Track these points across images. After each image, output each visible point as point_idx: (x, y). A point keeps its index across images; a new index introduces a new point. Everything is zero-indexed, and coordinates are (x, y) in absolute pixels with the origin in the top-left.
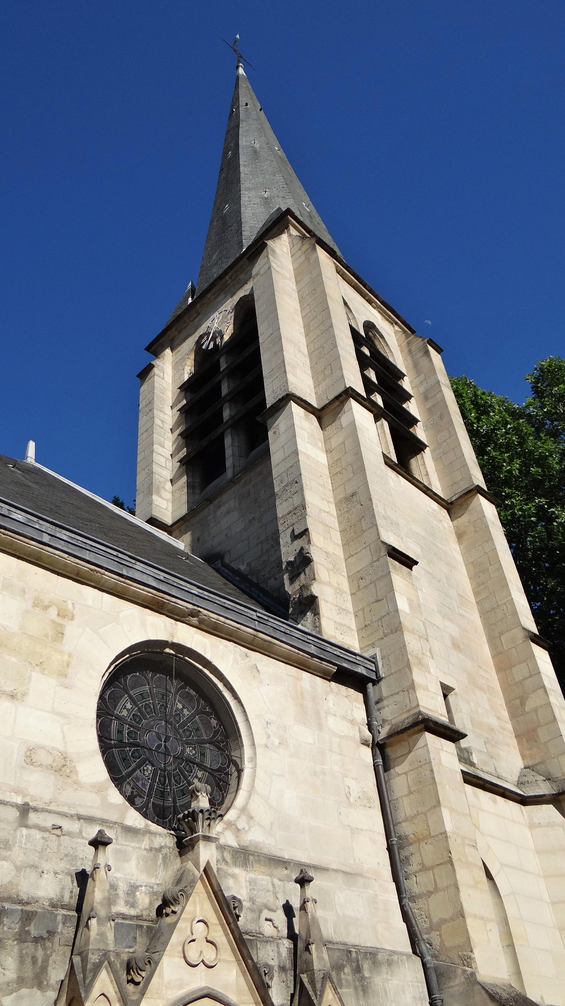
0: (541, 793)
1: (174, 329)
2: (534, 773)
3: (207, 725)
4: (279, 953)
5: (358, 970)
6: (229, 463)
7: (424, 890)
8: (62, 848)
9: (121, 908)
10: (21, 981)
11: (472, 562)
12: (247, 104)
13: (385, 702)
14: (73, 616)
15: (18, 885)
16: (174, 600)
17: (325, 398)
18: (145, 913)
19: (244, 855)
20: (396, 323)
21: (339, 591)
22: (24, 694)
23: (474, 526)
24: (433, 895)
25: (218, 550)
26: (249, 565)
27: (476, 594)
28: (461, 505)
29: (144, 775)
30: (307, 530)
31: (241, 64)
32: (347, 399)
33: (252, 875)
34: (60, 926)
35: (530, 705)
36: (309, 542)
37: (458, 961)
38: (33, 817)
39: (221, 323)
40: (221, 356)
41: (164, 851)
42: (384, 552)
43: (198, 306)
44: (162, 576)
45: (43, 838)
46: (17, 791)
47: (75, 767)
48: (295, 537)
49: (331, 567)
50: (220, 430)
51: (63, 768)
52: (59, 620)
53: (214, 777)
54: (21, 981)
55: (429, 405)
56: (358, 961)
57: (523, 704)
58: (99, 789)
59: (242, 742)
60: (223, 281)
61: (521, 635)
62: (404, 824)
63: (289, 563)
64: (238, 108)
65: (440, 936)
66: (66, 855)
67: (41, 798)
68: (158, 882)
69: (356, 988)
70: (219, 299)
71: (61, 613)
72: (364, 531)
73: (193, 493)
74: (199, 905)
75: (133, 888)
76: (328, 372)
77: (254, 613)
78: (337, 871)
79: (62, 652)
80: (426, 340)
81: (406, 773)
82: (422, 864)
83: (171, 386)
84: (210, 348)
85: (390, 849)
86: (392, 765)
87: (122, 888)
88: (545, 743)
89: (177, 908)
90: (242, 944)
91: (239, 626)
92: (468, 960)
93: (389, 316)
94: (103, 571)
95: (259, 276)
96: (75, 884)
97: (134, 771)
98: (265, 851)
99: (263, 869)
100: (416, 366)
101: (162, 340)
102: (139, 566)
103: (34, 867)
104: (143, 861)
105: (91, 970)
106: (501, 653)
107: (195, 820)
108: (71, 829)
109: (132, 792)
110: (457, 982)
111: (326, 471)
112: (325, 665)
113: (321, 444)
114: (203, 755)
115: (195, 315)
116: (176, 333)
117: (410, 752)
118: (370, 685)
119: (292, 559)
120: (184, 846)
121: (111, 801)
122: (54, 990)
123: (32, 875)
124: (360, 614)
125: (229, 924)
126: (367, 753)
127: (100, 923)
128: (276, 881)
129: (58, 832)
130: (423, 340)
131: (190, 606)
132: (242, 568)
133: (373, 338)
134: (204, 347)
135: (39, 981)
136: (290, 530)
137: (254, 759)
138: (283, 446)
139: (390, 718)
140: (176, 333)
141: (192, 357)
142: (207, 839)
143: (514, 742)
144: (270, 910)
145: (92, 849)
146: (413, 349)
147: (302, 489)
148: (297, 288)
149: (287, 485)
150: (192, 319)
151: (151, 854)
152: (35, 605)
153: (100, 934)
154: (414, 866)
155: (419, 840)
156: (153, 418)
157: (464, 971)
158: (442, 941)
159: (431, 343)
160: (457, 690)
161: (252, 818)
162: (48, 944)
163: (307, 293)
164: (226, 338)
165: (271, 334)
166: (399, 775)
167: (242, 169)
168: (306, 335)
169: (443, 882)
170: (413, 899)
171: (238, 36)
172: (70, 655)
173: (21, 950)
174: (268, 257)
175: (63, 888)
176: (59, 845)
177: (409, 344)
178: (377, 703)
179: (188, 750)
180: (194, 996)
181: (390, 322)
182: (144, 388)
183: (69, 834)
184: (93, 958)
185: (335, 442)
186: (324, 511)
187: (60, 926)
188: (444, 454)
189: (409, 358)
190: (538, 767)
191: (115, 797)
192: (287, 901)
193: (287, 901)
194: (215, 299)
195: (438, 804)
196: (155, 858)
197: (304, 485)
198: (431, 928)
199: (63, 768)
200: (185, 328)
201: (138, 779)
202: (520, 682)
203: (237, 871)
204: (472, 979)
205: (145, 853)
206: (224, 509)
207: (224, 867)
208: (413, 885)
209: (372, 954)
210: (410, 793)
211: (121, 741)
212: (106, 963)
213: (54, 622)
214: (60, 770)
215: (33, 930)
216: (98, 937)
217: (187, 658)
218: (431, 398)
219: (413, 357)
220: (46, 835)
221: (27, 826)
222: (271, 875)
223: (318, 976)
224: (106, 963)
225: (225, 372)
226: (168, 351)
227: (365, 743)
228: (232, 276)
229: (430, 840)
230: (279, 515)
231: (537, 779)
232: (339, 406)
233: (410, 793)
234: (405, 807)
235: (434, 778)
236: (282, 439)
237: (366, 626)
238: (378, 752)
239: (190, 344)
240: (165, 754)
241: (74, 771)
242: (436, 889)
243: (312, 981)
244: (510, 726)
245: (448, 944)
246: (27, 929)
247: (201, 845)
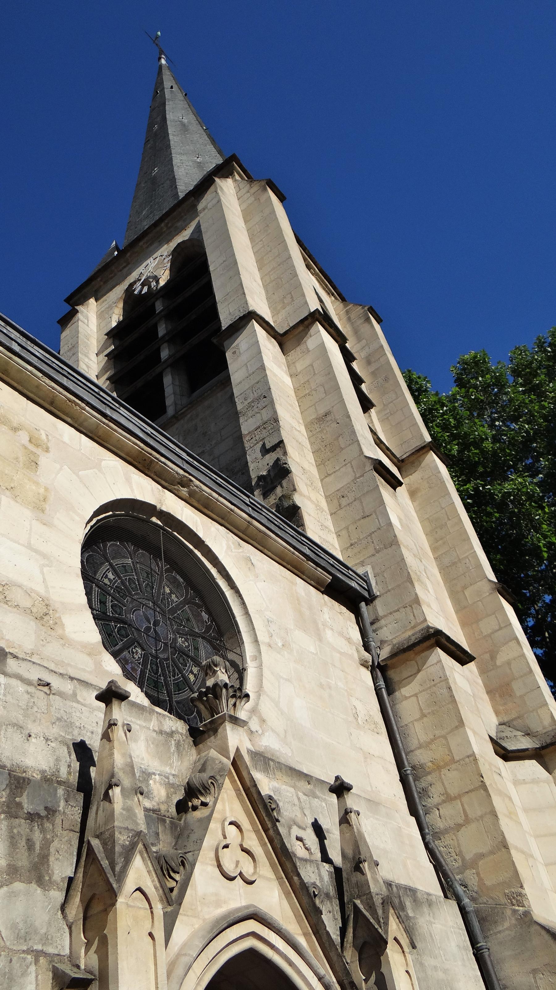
0: (524, 747)
1: (99, 279)
2: (510, 729)
3: (198, 617)
6: (169, 401)
7: (451, 823)
8: (53, 709)
12: (172, 87)
13: (383, 622)
16: (163, 459)
17: (286, 325)
18: (163, 808)
20: (333, 294)
21: (318, 507)
23: (428, 482)
24: (463, 829)
27: (434, 549)
28: (413, 463)
29: (133, 657)
30: (282, 442)
31: (163, 56)
32: (313, 323)
34: (62, 803)
35: (501, 659)
36: (285, 453)
37: (504, 900)
39: (157, 267)
40: (157, 299)
41: (177, 737)
42: (369, 466)
43: (129, 254)
44: (149, 430)
45: (28, 693)
47: (60, 618)
48: (265, 451)
49: (309, 483)
52: (31, 447)
54: (13, 872)
56: (400, 897)
57: (493, 657)
59: (242, 639)
60: (158, 229)
62: (418, 752)
63: (260, 478)
64: (163, 90)
65: (478, 874)
66: (59, 719)
67: (20, 646)
68: (173, 772)
70: (152, 248)
71: (33, 441)
72: (342, 449)
74: (228, 804)
76: (288, 300)
77: (247, 499)
79: (37, 483)
80: (366, 308)
81: (416, 695)
82: (446, 793)
83: (96, 334)
84: (143, 292)
85: (404, 780)
86: (396, 688)
88: (521, 696)
89: (208, 799)
90: (284, 858)
91: (233, 507)
92: (518, 898)
93: (326, 286)
94: (83, 405)
95: (206, 211)
96: (74, 756)
98: (282, 760)
99: (285, 778)
100: (356, 332)
101: (85, 290)
103: (19, 727)
104: (153, 743)
105: (121, 854)
106: (465, 607)
107: (217, 697)
108: (62, 689)
110: (507, 924)
111: (292, 393)
113: (285, 368)
114: (197, 649)
115: (125, 264)
116: (102, 283)
117: (419, 671)
118: (363, 604)
119: (265, 473)
120: (197, 736)
121: (106, 668)
122: (59, 889)
124: (344, 533)
125: (266, 831)
126: (366, 675)
128: (300, 794)
129: (46, 689)
130: (363, 308)
131: (181, 472)
134: (136, 292)
135: (38, 873)
137: (258, 657)
138: (246, 364)
139: (390, 638)
140: (102, 283)
141: (121, 305)
142: (235, 720)
143: (486, 697)
144: (300, 827)
145: (103, 705)
146: (353, 316)
147: (272, 403)
148: (246, 227)
149: (253, 402)
150: (121, 267)
151: (161, 738)
153: (125, 811)
155: (439, 768)
156: (78, 361)
157: (515, 911)
158: (481, 880)
159: (371, 310)
161: (264, 721)
162: (48, 825)
163: (259, 230)
164: (162, 283)
165: (224, 261)
166: (406, 698)
167: (171, 137)
168: (260, 269)
169: (475, 811)
170: (437, 835)
171: (159, 33)
172: (46, 489)
173: (11, 828)
174: (216, 192)
175: (58, 760)
176: (49, 705)
177: (347, 312)
178: (372, 623)
179: (180, 640)
180: (240, 914)
181: (326, 291)
182: (66, 334)
183: (61, 694)
184: (122, 839)
185: (300, 366)
186: (296, 429)
187: (62, 803)
188: (391, 414)
190: (515, 723)
192: (316, 819)
193: (316, 819)
194: (147, 247)
196: (166, 744)
197: (274, 399)
198: (461, 871)
200: (111, 278)
202: (489, 636)
204: (526, 919)
205: (154, 734)
208: (434, 820)
210: (423, 716)
211: (105, 613)
212: (140, 846)
214: (42, 618)
215: (27, 803)
216: (124, 812)
217: (175, 533)
218: (375, 362)
220: (31, 689)
222: (294, 787)
223: (378, 901)
224: (140, 846)
225: (163, 313)
226: (92, 301)
227: (364, 664)
229: (454, 766)
230: (244, 431)
231: (515, 734)
232: (303, 330)
233: (423, 716)
234: (417, 732)
235: (452, 696)
236: (244, 358)
237: (352, 545)
238: (379, 674)
239: (119, 291)
240: (155, 638)
242: (467, 821)
243: (371, 907)
244: (480, 682)
245: (488, 883)
246: (17, 799)
247: (228, 726)
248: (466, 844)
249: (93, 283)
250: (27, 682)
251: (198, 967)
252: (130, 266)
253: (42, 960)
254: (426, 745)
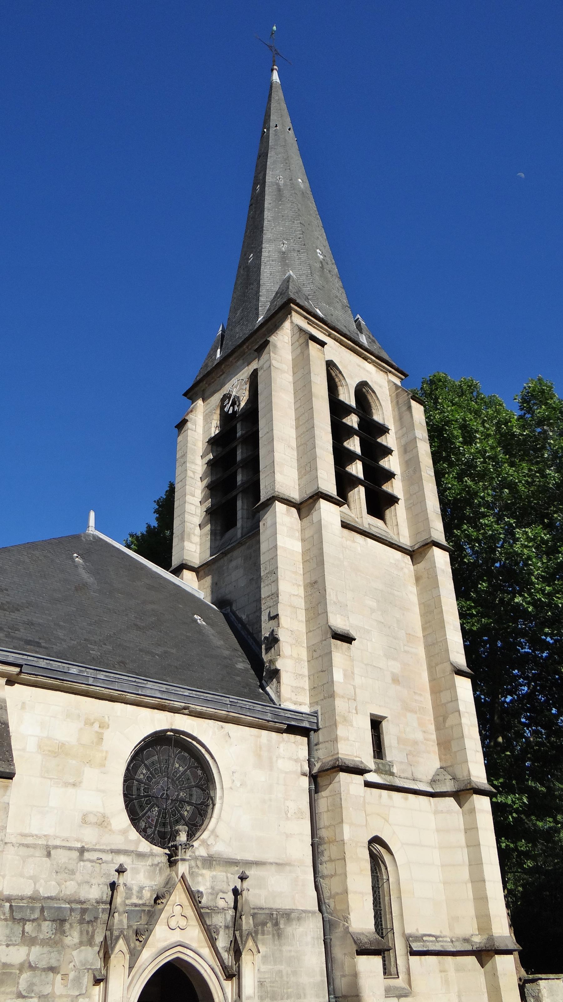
0: (445, 790)
1: (205, 382)
2: (445, 773)
3: (195, 775)
4: (225, 918)
5: (276, 924)
6: (239, 524)
8: (102, 870)
9: (135, 900)
10: (81, 943)
11: (423, 603)
12: (276, 126)
13: (320, 746)
14: (108, 726)
15: (79, 893)
16: (172, 702)
17: (305, 492)
18: (147, 902)
19: (210, 861)
20: (390, 372)
21: (298, 660)
22: (80, 782)
23: (428, 573)
24: (333, 877)
25: (228, 597)
26: (248, 616)
27: (424, 629)
28: (421, 553)
30: (278, 615)
31: (275, 67)
32: (317, 499)
33: (214, 873)
34: (101, 914)
35: (449, 723)
36: (278, 626)
37: (342, 918)
38: (87, 855)
40: (238, 422)
41: (160, 865)
42: (329, 635)
43: (223, 366)
44: (164, 688)
45: (92, 866)
46: (78, 840)
49: (294, 642)
50: (234, 493)
51: (103, 823)
52: (100, 730)
53: (197, 808)
54: (81, 943)
55: (407, 457)
56: (277, 919)
57: (444, 721)
58: (124, 832)
59: (216, 786)
60: (242, 349)
61: (449, 668)
62: (323, 830)
63: (265, 638)
65: (335, 902)
66: (104, 874)
69: (273, 935)
71: (101, 726)
72: (319, 614)
73: (215, 540)
74: (179, 896)
75: (141, 889)
76: (308, 469)
77: (228, 699)
78: (271, 864)
80: (410, 396)
81: (327, 797)
82: (330, 857)
83: (202, 436)
84: (230, 413)
85: (313, 845)
86: (320, 790)
87: (135, 889)
88: (455, 752)
89: (164, 901)
90: (202, 915)
91: (216, 711)
92: (346, 919)
93: (384, 367)
94: (126, 694)
96: (109, 889)
97: (146, 812)
98: (225, 856)
99: (221, 869)
102: (150, 685)
103: (88, 882)
105: (115, 939)
106: (435, 679)
107: (177, 849)
108: (107, 859)
109: (145, 826)
110: (340, 930)
111: (300, 557)
112: (278, 725)
113: (298, 534)
114: (191, 795)
115: (221, 373)
116: (207, 385)
117: (330, 783)
118: (312, 732)
119: (268, 635)
120: (172, 862)
123: (86, 887)
124: (312, 677)
125: (195, 906)
126: (305, 781)
127: (119, 915)
128: (229, 875)
129: (100, 861)
130: (408, 395)
131: (183, 704)
132: (244, 617)
133: (366, 393)
135: (90, 943)
136: (268, 611)
137: (222, 798)
139: (322, 758)
140: (207, 385)
142: (183, 860)
144: (224, 892)
145: (117, 873)
146: (400, 402)
147: (277, 580)
148: (294, 379)
151: (152, 868)
152: (86, 724)
153: (120, 920)
154: (325, 858)
155: (330, 842)
156: (186, 470)
157: (344, 925)
158: (335, 905)
160: (389, 718)
162: (95, 924)
164: (243, 404)
166: (323, 797)
167: (266, 213)
168: (297, 428)
169: (339, 871)
170: (323, 877)
171: (275, 28)
172: (107, 752)
173: (81, 929)
174: (269, 353)
175: (103, 893)
176: (101, 869)
177: (397, 395)
178: (316, 745)
179: (181, 794)
181: (384, 371)
182: (180, 439)
183: (106, 862)
184: (116, 933)
186: (294, 595)
187: (101, 914)
188: (414, 505)
189: (396, 409)
190: (449, 769)
191: (134, 834)
192: (236, 887)
193: (236, 887)
195: (342, 822)
196: (154, 871)
197: (279, 577)
199: (103, 823)
200: (213, 382)
201: (149, 817)
202: (445, 704)
205: (149, 867)
206: (234, 564)
207: (197, 870)
208: (324, 869)
209: (287, 915)
210: (328, 811)
211: (139, 795)
212: (122, 935)
213: (97, 732)
215: (87, 918)
217: (181, 736)
218: (409, 452)
219: (399, 409)
220: (94, 864)
221: (83, 861)
223: (245, 933)
224: (122, 935)
225: (240, 440)
226: (200, 402)
228: (248, 346)
229: (335, 843)
230: (263, 596)
231: (446, 778)
232: (312, 503)
233: (328, 811)
234: (324, 820)
235: (341, 804)
237: (314, 688)
238: (312, 780)
239: (216, 398)
240: (167, 799)
241: (109, 824)
243: (241, 936)
244: (434, 737)
245: (338, 908)
247: (180, 864)
248: (331, 886)
249: (201, 384)
250: (91, 861)
251: (147, 971)
252: (225, 375)
253: (90, 971)
254: (327, 827)
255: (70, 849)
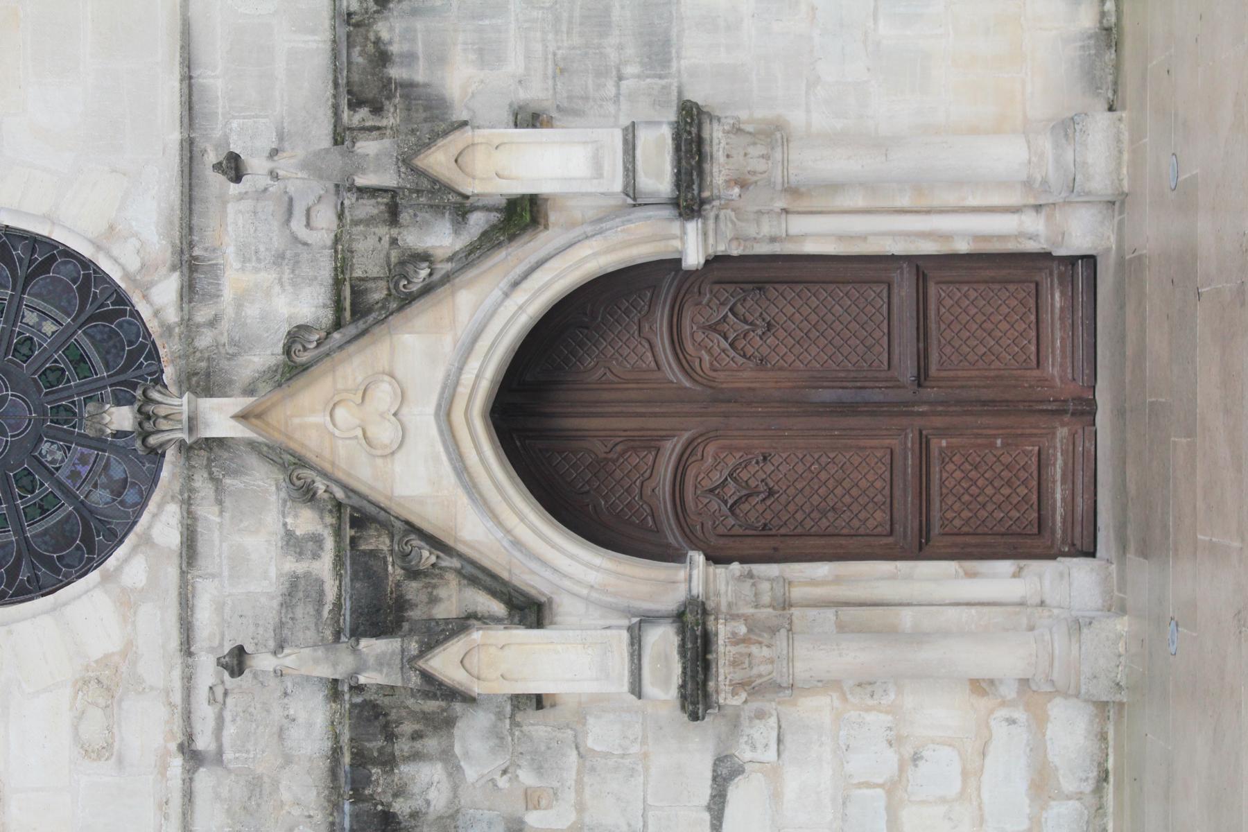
4: (369, 221)
10: (447, 756)
15: (311, 759)
29: (63, 461)
33: (231, 250)
46: (163, 768)
47: (96, 662)
51: (105, 683)
53: (28, 279)
58: (128, 603)
68: (274, 488)
87: (292, 565)
97: (60, 485)
103: (281, 732)
104: (241, 521)
109: (104, 487)
121: (144, 582)
123: (295, 733)
129: (219, 691)
151: (228, 503)
161: (111, 228)
162: (393, 715)
199: (105, 683)
201: (74, 475)
203: (228, 294)
205: (227, 515)
207: (225, 325)
214: (108, 689)
221: (220, 752)
241: (104, 661)
246: (376, 754)
253: (518, 718)
255: (189, 796)
